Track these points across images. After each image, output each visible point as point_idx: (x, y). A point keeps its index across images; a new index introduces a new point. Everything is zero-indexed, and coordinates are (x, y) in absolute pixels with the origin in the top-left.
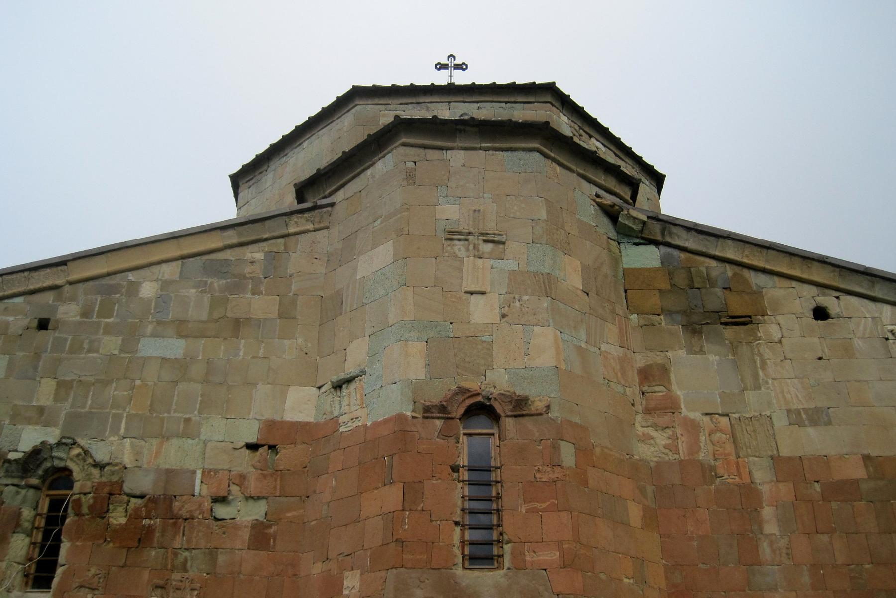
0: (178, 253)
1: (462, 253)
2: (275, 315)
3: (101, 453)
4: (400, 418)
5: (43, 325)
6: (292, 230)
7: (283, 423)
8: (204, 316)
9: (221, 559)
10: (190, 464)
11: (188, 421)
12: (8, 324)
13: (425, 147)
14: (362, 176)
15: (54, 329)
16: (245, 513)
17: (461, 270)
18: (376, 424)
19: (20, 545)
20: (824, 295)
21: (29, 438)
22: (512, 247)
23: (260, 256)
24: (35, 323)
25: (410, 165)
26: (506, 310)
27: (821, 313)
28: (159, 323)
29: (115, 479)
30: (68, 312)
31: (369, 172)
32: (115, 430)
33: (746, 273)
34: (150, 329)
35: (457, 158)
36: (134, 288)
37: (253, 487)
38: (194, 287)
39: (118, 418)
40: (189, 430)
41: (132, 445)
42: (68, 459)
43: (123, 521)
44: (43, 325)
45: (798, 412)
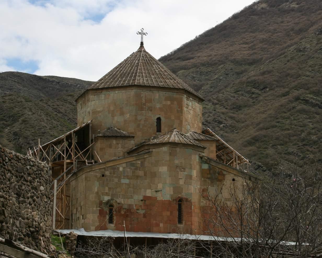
0: (126, 161)
1: (179, 171)
2: (143, 175)
3: (118, 201)
4: (169, 201)
5: (103, 176)
6: (145, 157)
7: (147, 196)
8: (132, 175)
9: (139, 219)
10: (133, 203)
11: (131, 195)
12: (97, 175)
13: (173, 147)
14: (159, 148)
15: (106, 177)
16: (142, 212)
17: (178, 174)
18: (164, 200)
19: (108, 217)
20: (235, 176)
21: (106, 198)
22: (187, 170)
23: (140, 162)
24: (102, 176)
25: (170, 151)
26: (185, 182)
27: (234, 180)
28: (124, 176)
29: (121, 206)
30: (107, 173)
31: (161, 148)
32: (120, 197)
33: (222, 171)
34: (122, 177)
35: (178, 149)
36: (118, 168)
37: (143, 208)
38: (129, 169)
39: (120, 195)
40: (132, 197)
41: (123, 200)
42: (113, 202)
43: (123, 213)
44: (103, 176)
45: (226, 198)
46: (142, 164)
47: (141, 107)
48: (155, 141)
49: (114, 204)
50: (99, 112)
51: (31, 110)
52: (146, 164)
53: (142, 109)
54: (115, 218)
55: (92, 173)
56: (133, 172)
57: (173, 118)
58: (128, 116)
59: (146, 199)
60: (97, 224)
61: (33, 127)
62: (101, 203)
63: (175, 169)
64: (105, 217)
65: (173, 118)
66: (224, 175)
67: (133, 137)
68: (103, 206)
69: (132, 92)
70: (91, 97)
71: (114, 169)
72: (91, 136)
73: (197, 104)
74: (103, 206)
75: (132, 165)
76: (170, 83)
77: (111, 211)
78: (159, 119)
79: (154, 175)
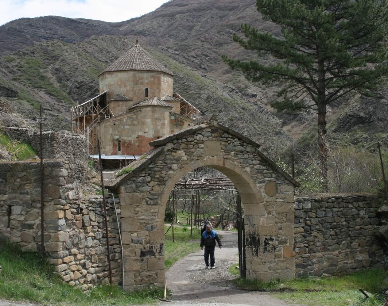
16: (137, 144)
19: (118, 147)
21: (116, 137)
22: (162, 120)
27: (189, 125)
30: (117, 123)
35: (157, 109)
36: (123, 120)
40: (131, 136)
42: (120, 139)
46: (136, 117)
47: (136, 82)
48: (144, 104)
49: (121, 140)
50: (112, 85)
51: (67, 51)
52: (139, 117)
53: (137, 84)
54: (122, 148)
55: (108, 123)
56: (132, 122)
57: (155, 88)
58: (128, 88)
59: (139, 137)
60: (112, 151)
61: (69, 65)
62: (114, 140)
63: (155, 120)
64: (116, 147)
65: (155, 88)
66: (183, 122)
67: (132, 100)
68: (115, 141)
69: (131, 74)
70: (107, 76)
71: (121, 120)
72: (108, 99)
73: (170, 79)
74: (115, 141)
75: (131, 118)
76: (154, 67)
77: (119, 144)
78: (147, 89)
79: (143, 123)
